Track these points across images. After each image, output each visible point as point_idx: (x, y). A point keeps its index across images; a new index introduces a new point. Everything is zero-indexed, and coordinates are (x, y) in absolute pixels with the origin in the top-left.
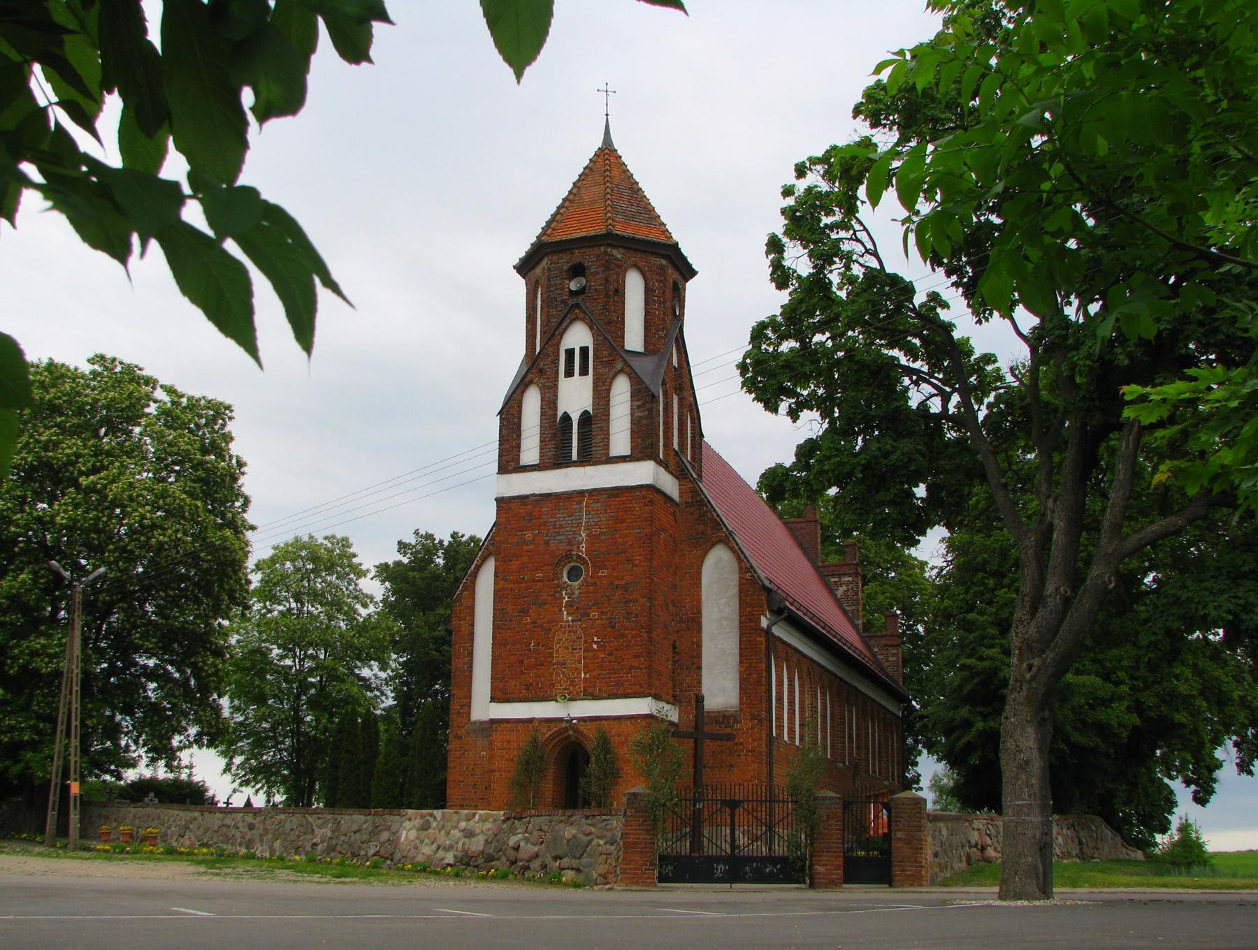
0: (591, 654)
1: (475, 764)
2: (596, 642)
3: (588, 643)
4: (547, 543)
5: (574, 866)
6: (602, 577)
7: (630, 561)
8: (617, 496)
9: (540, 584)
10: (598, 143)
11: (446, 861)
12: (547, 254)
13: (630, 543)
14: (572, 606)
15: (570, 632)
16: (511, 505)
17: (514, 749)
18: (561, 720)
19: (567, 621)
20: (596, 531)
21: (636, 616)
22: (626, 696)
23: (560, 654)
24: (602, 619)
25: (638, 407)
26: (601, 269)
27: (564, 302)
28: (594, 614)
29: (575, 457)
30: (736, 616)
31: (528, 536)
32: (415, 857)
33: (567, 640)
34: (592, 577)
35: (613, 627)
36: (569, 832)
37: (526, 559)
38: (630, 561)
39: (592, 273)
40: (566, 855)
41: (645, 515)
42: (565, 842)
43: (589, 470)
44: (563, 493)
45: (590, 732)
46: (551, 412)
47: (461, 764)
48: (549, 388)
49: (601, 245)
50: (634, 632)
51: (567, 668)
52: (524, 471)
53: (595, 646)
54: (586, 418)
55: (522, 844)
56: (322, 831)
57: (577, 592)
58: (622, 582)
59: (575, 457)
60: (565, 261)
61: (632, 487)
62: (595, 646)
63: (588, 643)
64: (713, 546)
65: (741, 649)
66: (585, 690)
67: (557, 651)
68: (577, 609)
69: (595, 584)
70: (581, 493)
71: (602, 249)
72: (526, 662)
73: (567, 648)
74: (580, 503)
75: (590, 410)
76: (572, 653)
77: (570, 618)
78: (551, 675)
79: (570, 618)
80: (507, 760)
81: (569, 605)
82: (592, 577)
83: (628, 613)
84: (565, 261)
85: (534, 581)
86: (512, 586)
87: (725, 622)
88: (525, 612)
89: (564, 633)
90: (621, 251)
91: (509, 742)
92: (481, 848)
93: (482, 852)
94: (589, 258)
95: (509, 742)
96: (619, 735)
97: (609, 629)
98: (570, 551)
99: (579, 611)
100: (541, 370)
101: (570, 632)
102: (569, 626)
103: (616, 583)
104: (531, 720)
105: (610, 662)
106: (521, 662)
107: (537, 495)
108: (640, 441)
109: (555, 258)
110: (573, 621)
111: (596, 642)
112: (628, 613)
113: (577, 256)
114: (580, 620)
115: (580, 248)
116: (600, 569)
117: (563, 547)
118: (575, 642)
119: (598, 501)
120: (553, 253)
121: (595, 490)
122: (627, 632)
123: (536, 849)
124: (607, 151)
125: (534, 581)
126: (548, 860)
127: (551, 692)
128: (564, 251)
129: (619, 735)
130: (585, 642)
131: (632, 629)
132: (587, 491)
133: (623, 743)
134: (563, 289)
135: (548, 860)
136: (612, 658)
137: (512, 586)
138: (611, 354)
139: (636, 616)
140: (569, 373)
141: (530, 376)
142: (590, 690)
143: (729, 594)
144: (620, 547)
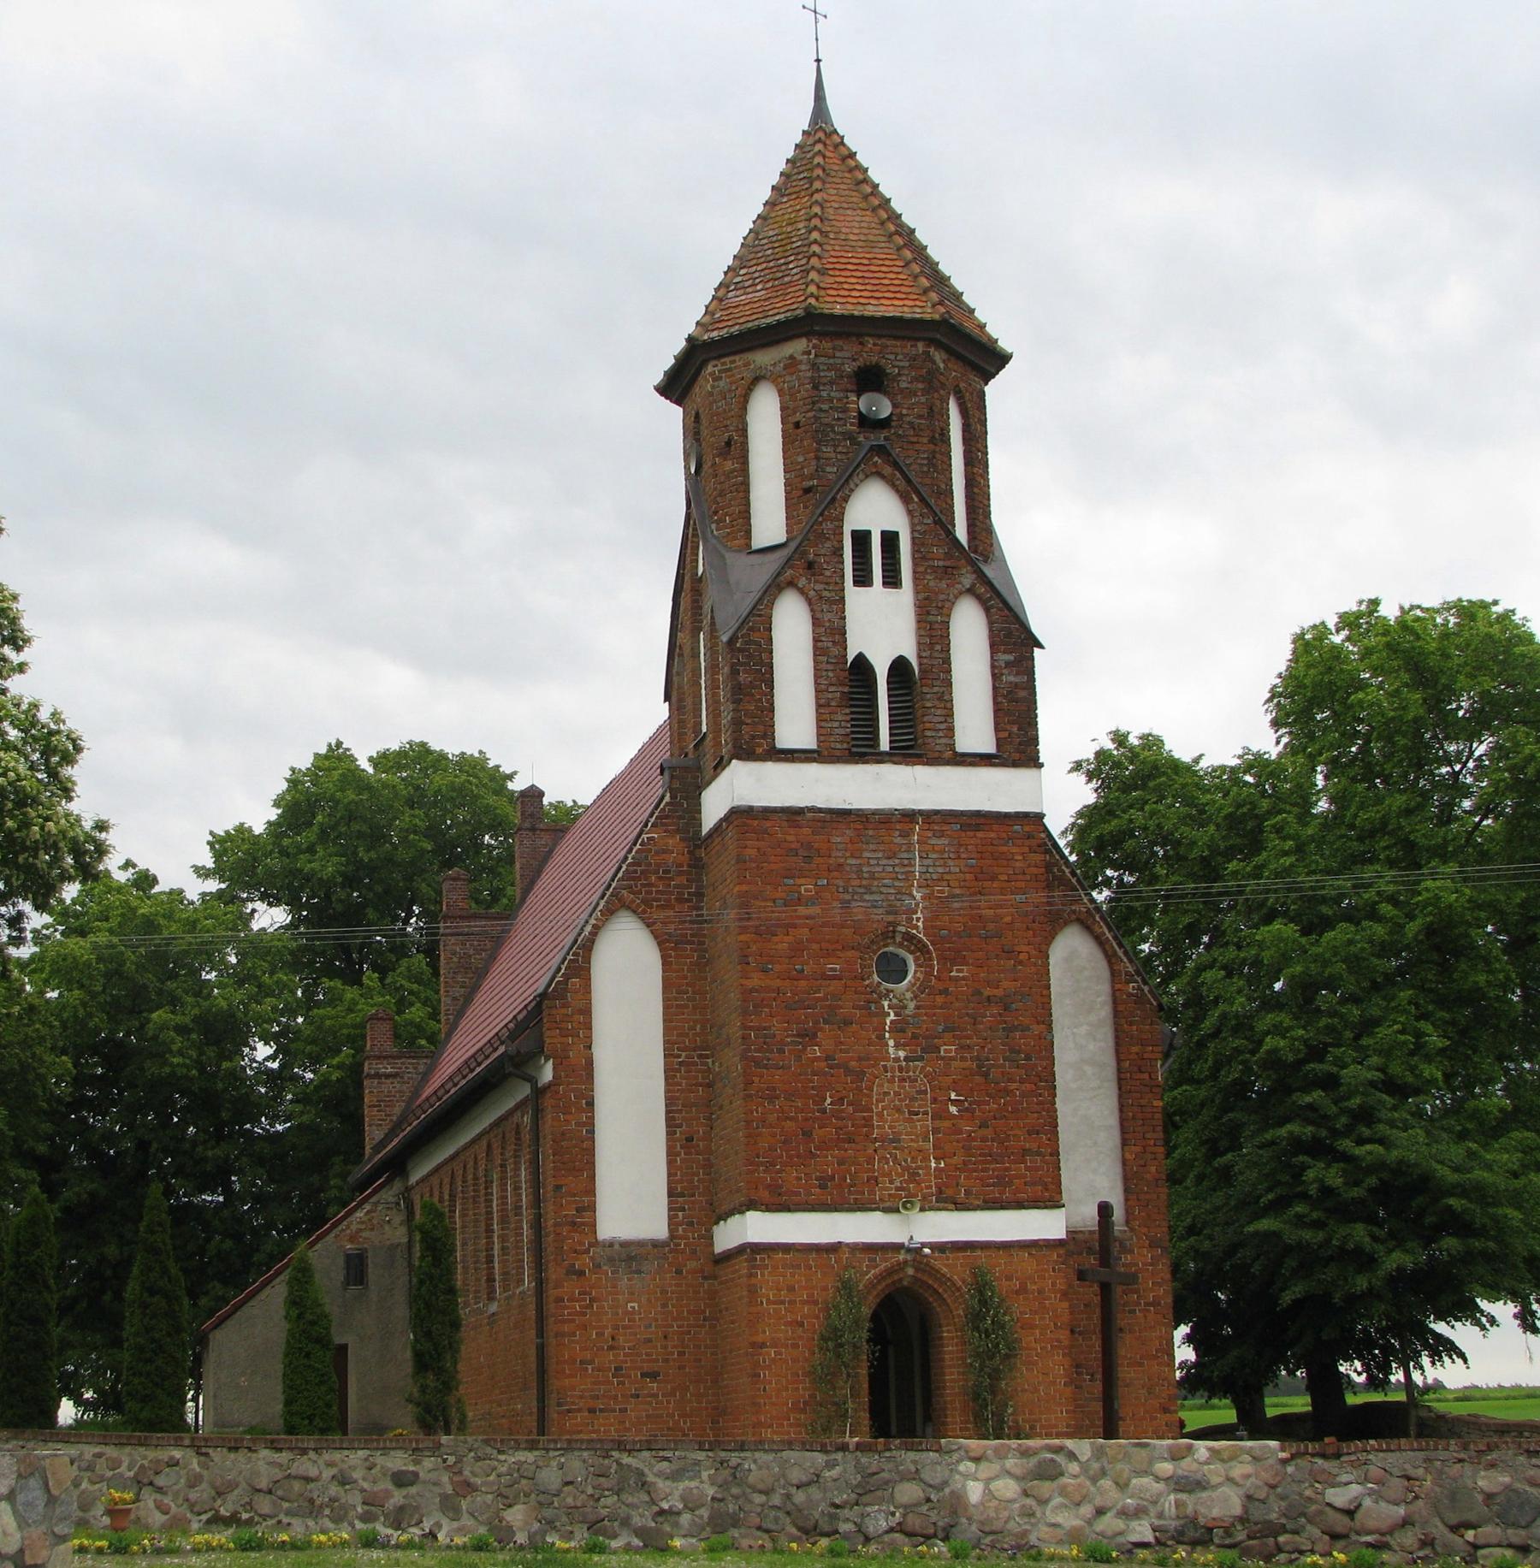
0: (947, 1124)
1: (616, 1327)
2: (955, 1102)
3: (940, 1103)
4: (846, 905)
5: (1516, 1540)
6: (957, 979)
7: (1009, 953)
8: (977, 828)
9: (835, 986)
10: (802, 120)
11: (1134, 1538)
12: (808, 335)
13: (1008, 919)
14: (902, 1031)
15: (903, 1080)
16: (768, 824)
17: (804, 1303)
18: (897, 1247)
19: (897, 1059)
20: (942, 890)
21: (1028, 1058)
22: (1019, 1205)
23: (886, 1122)
24: (963, 1059)
25: (1008, 664)
26: (920, 386)
27: (850, 437)
28: (948, 1049)
29: (884, 744)
30: (1109, 1059)
31: (806, 888)
32: (1025, 1533)
33: (897, 1094)
34: (938, 978)
35: (986, 1075)
36: (1487, 1481)
37: (804, 933)
38: (1009, 953)
39: (902, 391)
40: (1486, 1521)
41: (1034, 870)
42: (1480, 1498)
43: (922, 772)
44: (875, 812)
45: (955, 1270)
46: (835, 651)
47: (585, 1327)
48: (831, 602)
49: (918, 339)
50: (1028, 1086)
51: (902, 1149)
52: (793, 761)
53: (953, 1110)
54: (899, 667)
55: (1367, 1502)
56: (682, 1486)
57: (912, 1005)
58: (999, 992)
59: (884, 744)
60: (849, 357)
61: (1007, 816)
62: (953, 1110)
63: (940, 1103)
64: (1066, 924)
65: (1123, 1122)
66: (940, 1192)
67: (880, 1115)
68: (915, 1036)
69: (945, 992)
70: (909, 816)
71: (921, 346)
72: (818, 1133)
73: (898, 1110)
74: (906, 834)
75: (911, 653)
76: (910, 1121)
77: (902, 1054)
78: (870, 1161)
79: (902, 1054)
80: (787, 1324)
81: (897, 1028)
82: (938, 978)
83: (1012, 1050)
84: (849, 357)
85: (825, 977)
86: (778, 983)
87: (1089, 1070)
88: (808, 1036)
89: (891, 1081)
90: (944, 356)
91: (791, 1289)
92: (1237, 1510)
93: (1243, 1520)
94: (895, 357)
95: (791, 1289)
96: (1009, 1278)
97: (978, 1078)
98: (895, 924)
99: (921, 1043)
100: (810, 566)
101: (903, 1080)
102: (901, 1069)
103: (987, 992)
104: (835, 1248)
105: (984, 1140)
106: (807, 1134)
107: (820, 810)
108: (1015, 729)
109: (827, 345)
110: (906, 1059)
111: (955, 1102)
112: (1012, 1050)
113: (871, 351)
114: (921, 1059)
115: (880, 336)
116: (954, 962)
117: (879, 915)
118: (913, 1099)
119: (942, 835)
120: (822, 335)
121: (937, 812)
122: (1014, 1086)
123: (1401, 1511)
124: (820, 135)
125: (825, 977)
126: (1438, 1530)
127: (872, 1192)
128: (845, 335)
129: (1009, 1278)
130: (934, 1100)
131: (1022, 1081)
132: (921, 812)
133: (1017, 1292)
134: (845, 410)
135: (1438, 1530)
136: (989, 1133)
137: (778, 983)
138: (948, 556)
139: (1028, 1058)
140: (863, 579)
141: (789, 572)
142: (949, 1192)
143: (1093, 1018)
144: (991, 926)
